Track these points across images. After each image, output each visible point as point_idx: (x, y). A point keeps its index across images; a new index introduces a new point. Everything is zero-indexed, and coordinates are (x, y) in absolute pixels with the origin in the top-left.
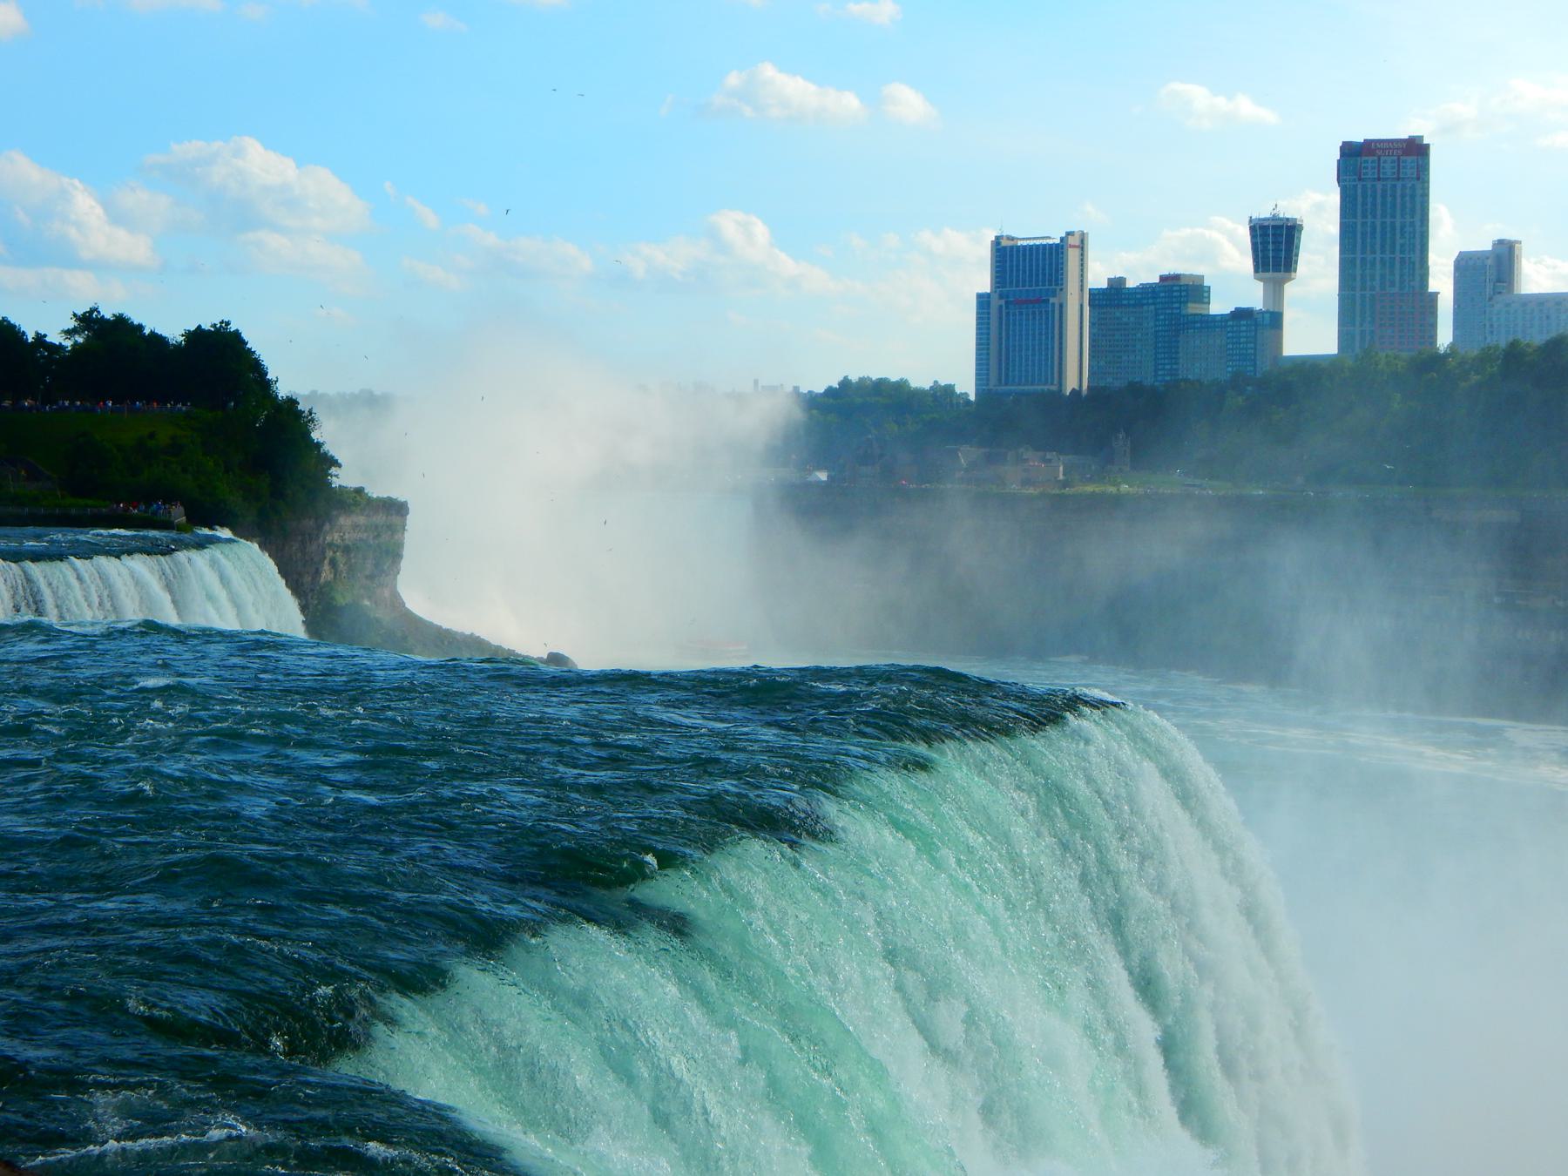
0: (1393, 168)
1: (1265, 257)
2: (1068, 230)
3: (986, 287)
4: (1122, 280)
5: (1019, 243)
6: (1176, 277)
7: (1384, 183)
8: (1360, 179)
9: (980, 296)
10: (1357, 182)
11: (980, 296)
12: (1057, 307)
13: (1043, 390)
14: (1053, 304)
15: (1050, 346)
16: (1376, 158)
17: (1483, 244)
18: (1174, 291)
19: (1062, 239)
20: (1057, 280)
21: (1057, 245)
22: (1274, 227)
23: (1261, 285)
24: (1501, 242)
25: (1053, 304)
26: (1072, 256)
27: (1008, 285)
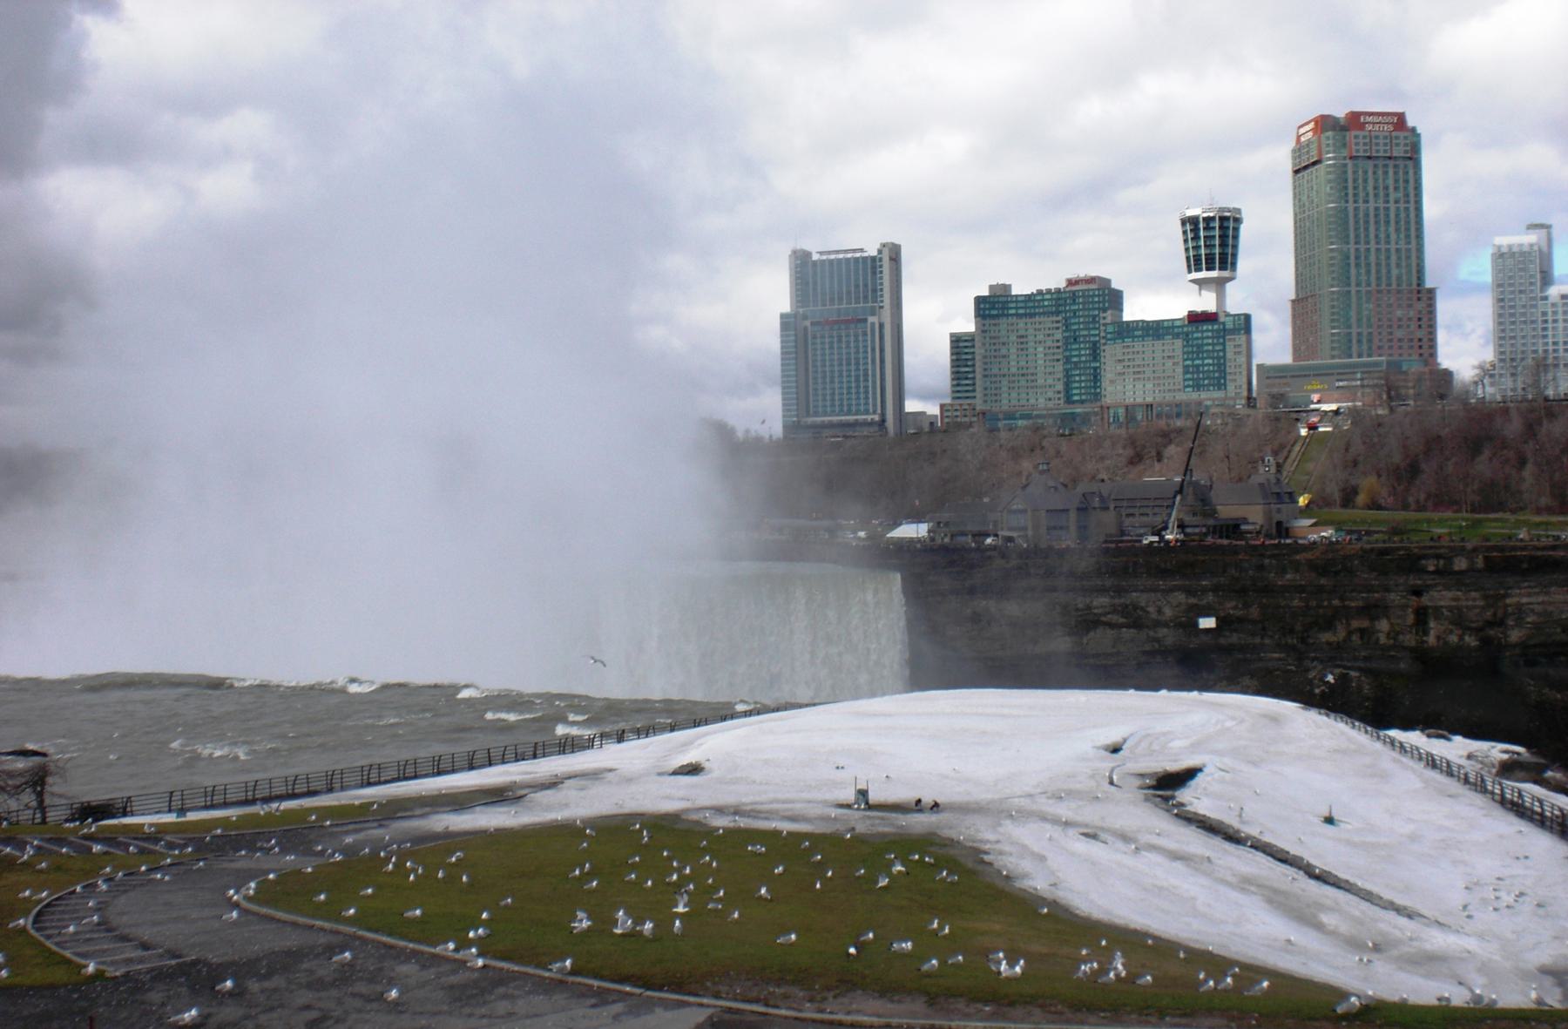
0: (1385, 144)
2: (884, 241)
4: (1007, 287)
7: (1376, 162)
10: (1348, 161)
11: (783, 316)
12: (877, 326)
13: (823, 421)
14: (873, 324)
15: (870, 372)
16: (1367, 133)
18: (1008, 308)
19: (880, 252)
21: (873, 259)
22: (1208, 220)
25: (873, 324)
27: (811, 304)
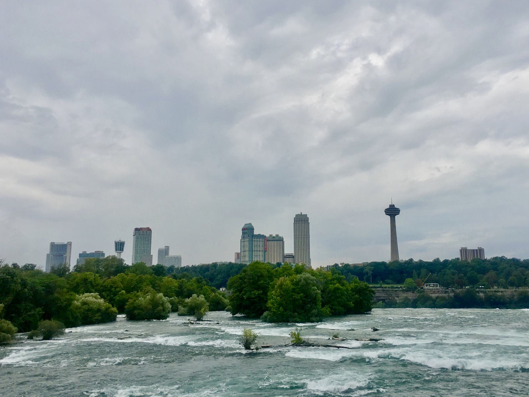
1: (118, 249)
3: (49, 253)
4: (85, 252)
5: (56, 244)
6: (99, 251)
8: (140, 235)
9: (47, 254)
11: (47, 254)
14: (64, 256)
17: (163, 247)
19: (67, 243)
20: (65, 251)
21: (66, 244)
23: (117, 253)
24: (166, 246)
25: (64, 256)
26: (68, 246)
